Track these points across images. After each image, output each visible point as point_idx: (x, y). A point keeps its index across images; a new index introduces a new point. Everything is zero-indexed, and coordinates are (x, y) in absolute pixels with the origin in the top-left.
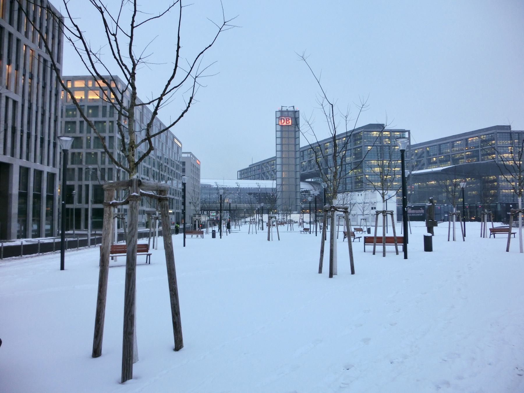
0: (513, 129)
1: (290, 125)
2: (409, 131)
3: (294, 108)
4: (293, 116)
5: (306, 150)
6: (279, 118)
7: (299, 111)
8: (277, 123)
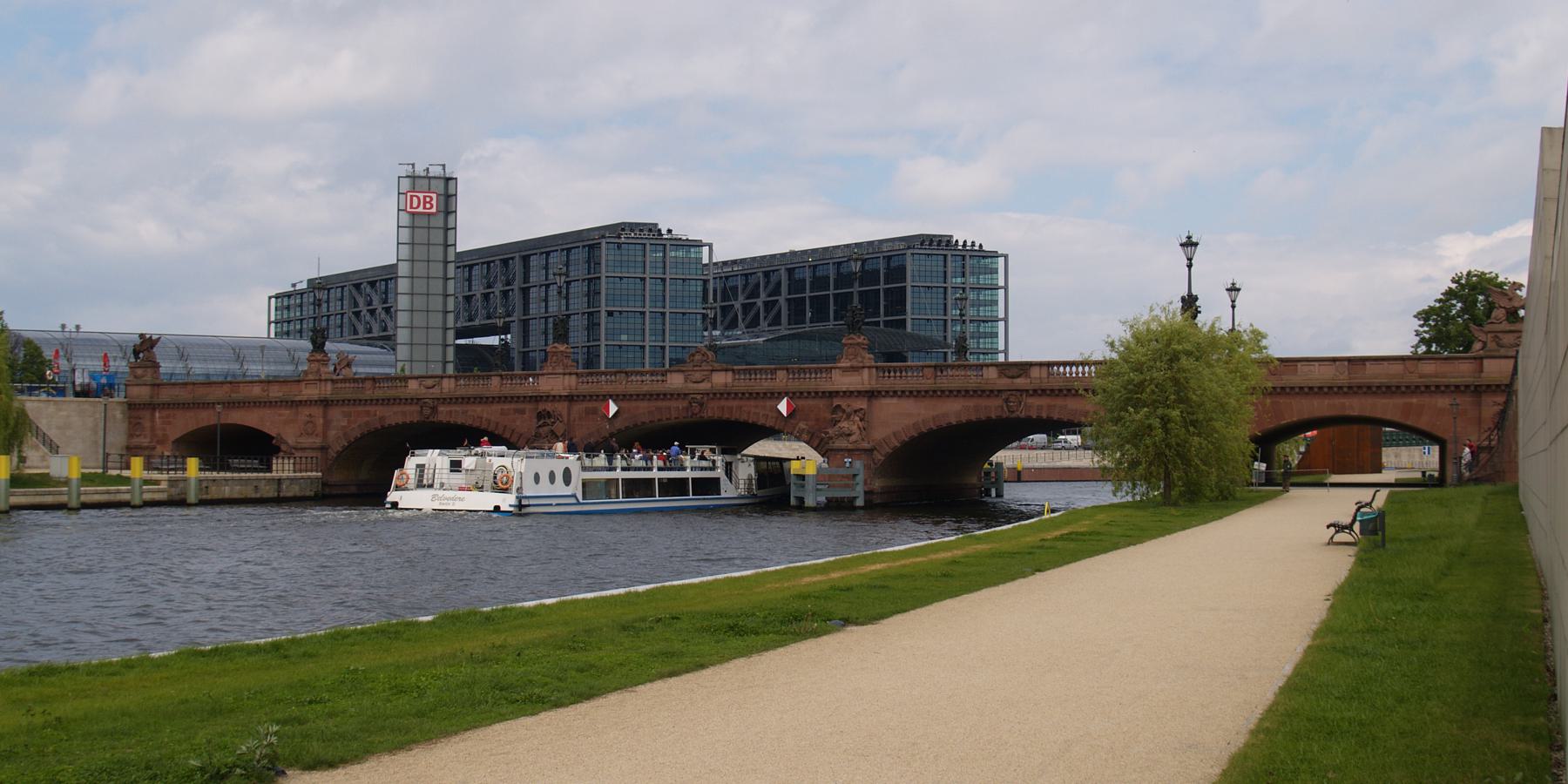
1: (432, 214)
3: (444, 169)
5: (477, 264)
6: (405, 194)
7: (456, 179)
8: (402, 207)
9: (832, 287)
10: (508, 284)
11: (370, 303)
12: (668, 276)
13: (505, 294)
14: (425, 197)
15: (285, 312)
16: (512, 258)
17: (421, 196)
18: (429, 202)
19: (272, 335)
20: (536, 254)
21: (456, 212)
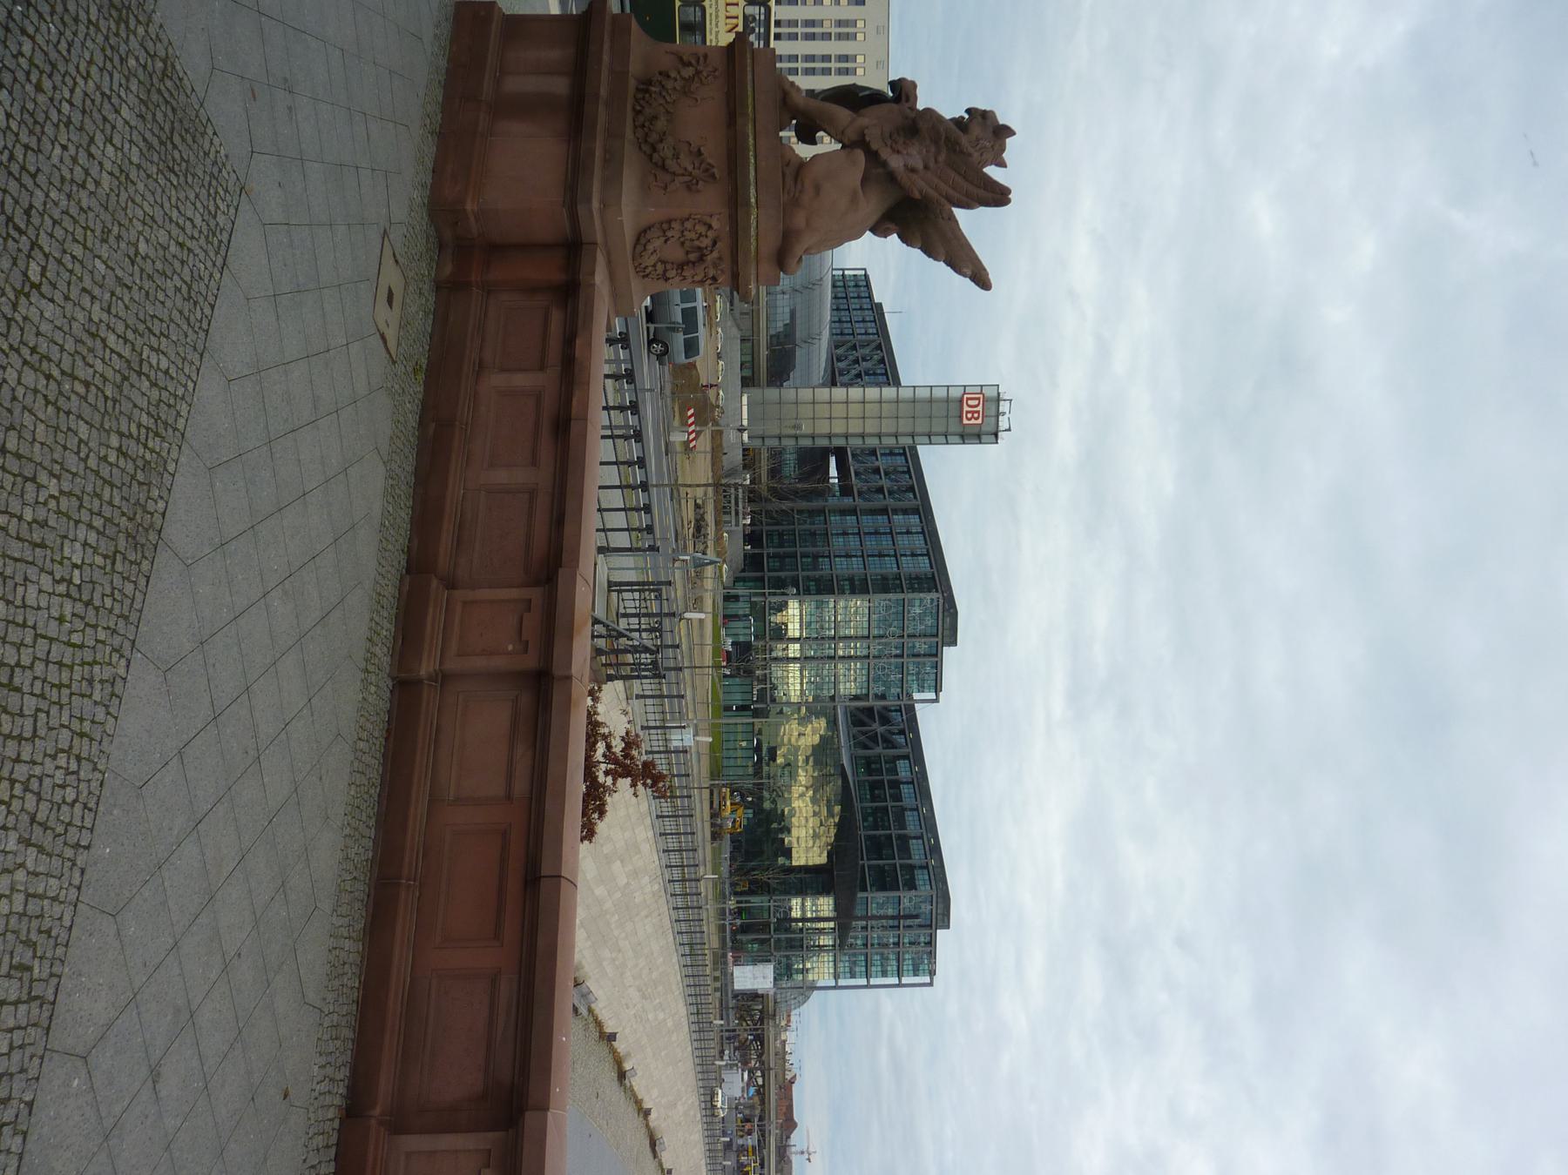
0: (941, 934)
2: (936, 700)
4: (984, 429)
8: (968, 390)
9: (902, 861)
10: (890, 493)
11: (864, 360)
12: (905, 660)
13: (880, 490)
14: (978, 412)
15: (852, 284)
16: (915, 497)
17: (980, 408)
18: (973, 417)
19: (834, 273)
20: (921, 522)
21: (964, 443)
